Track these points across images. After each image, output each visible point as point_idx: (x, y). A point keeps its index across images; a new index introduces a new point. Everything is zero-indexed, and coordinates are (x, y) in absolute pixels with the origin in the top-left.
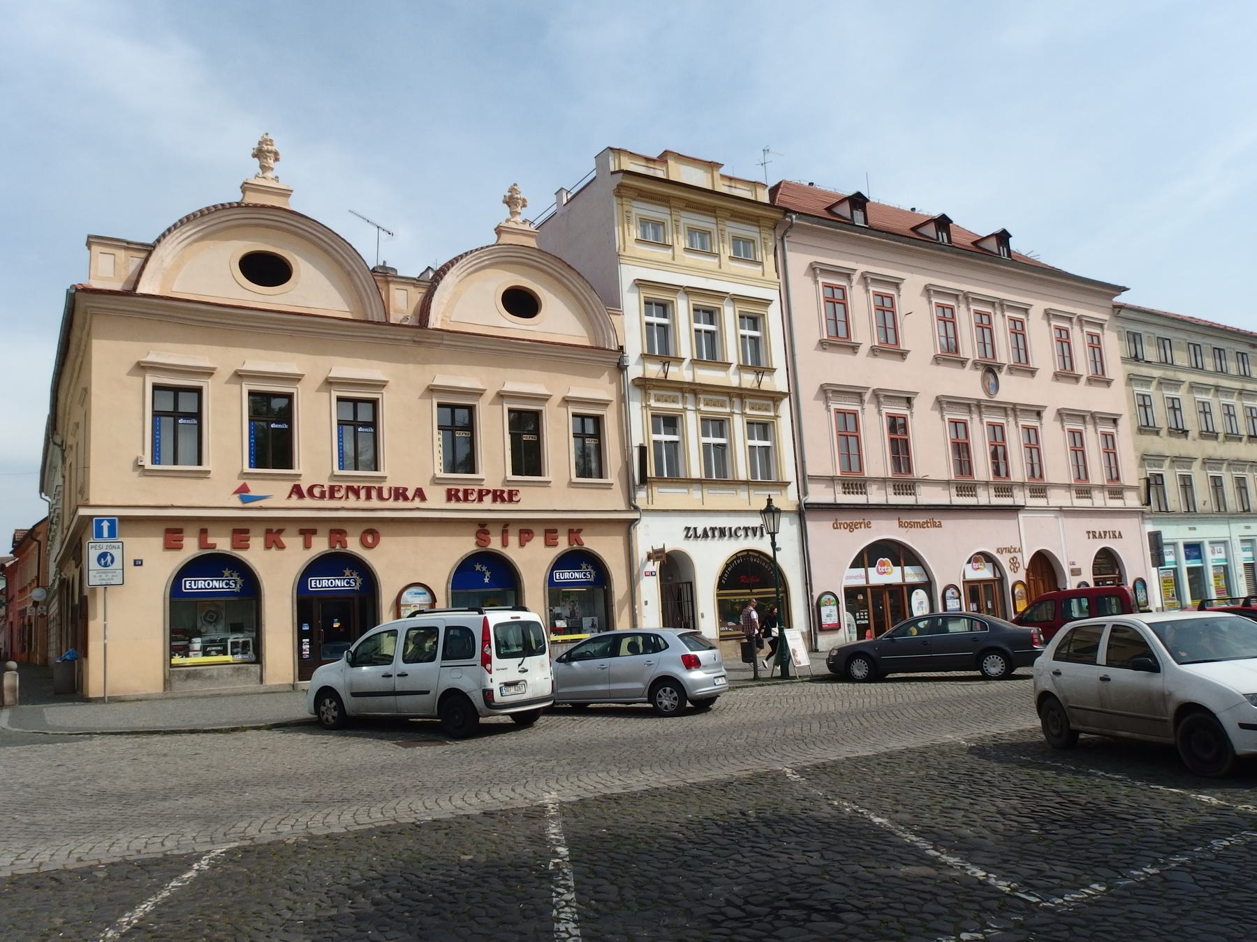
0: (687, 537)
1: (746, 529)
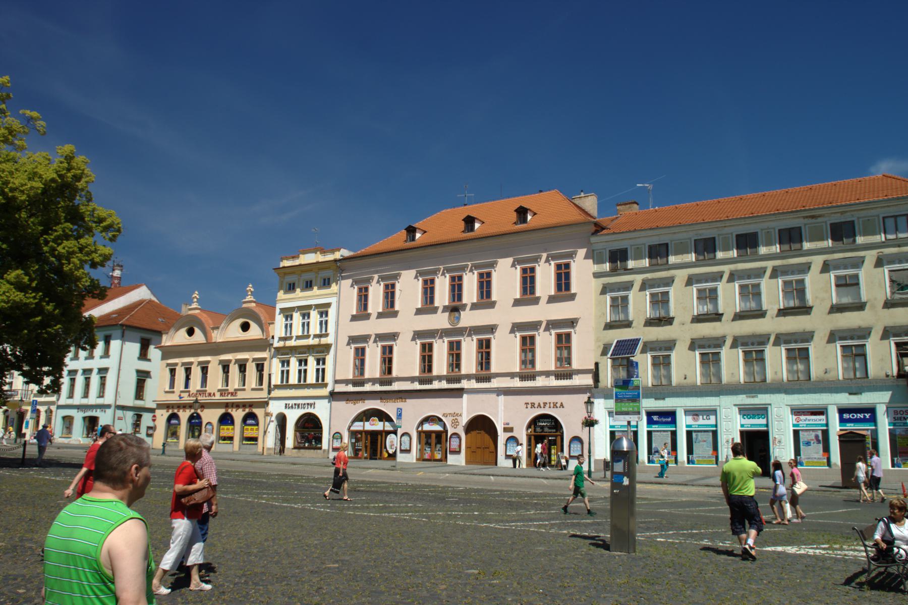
0: (286, 407)
1: (308, 404)
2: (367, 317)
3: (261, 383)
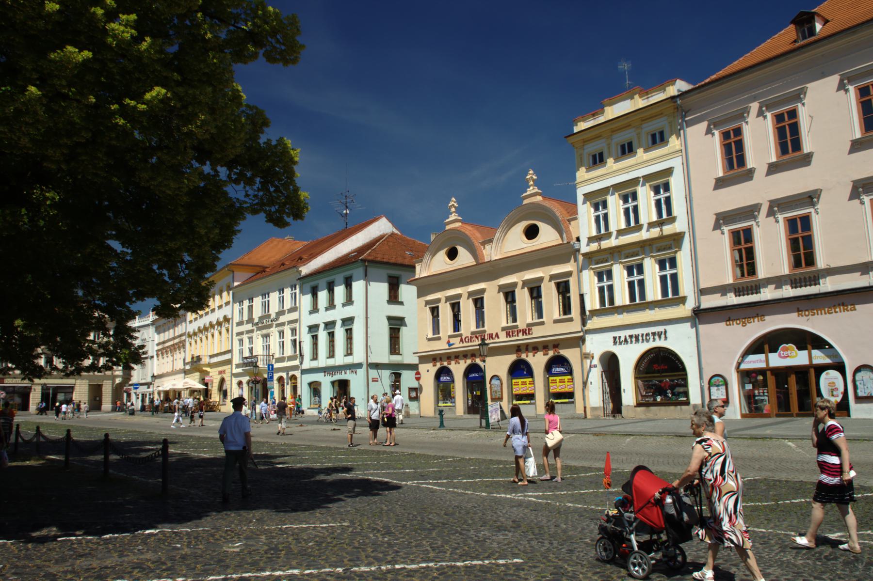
0: (615, 343)
1: (654, 334)
2: (749, 175)
3: (566, 308)
